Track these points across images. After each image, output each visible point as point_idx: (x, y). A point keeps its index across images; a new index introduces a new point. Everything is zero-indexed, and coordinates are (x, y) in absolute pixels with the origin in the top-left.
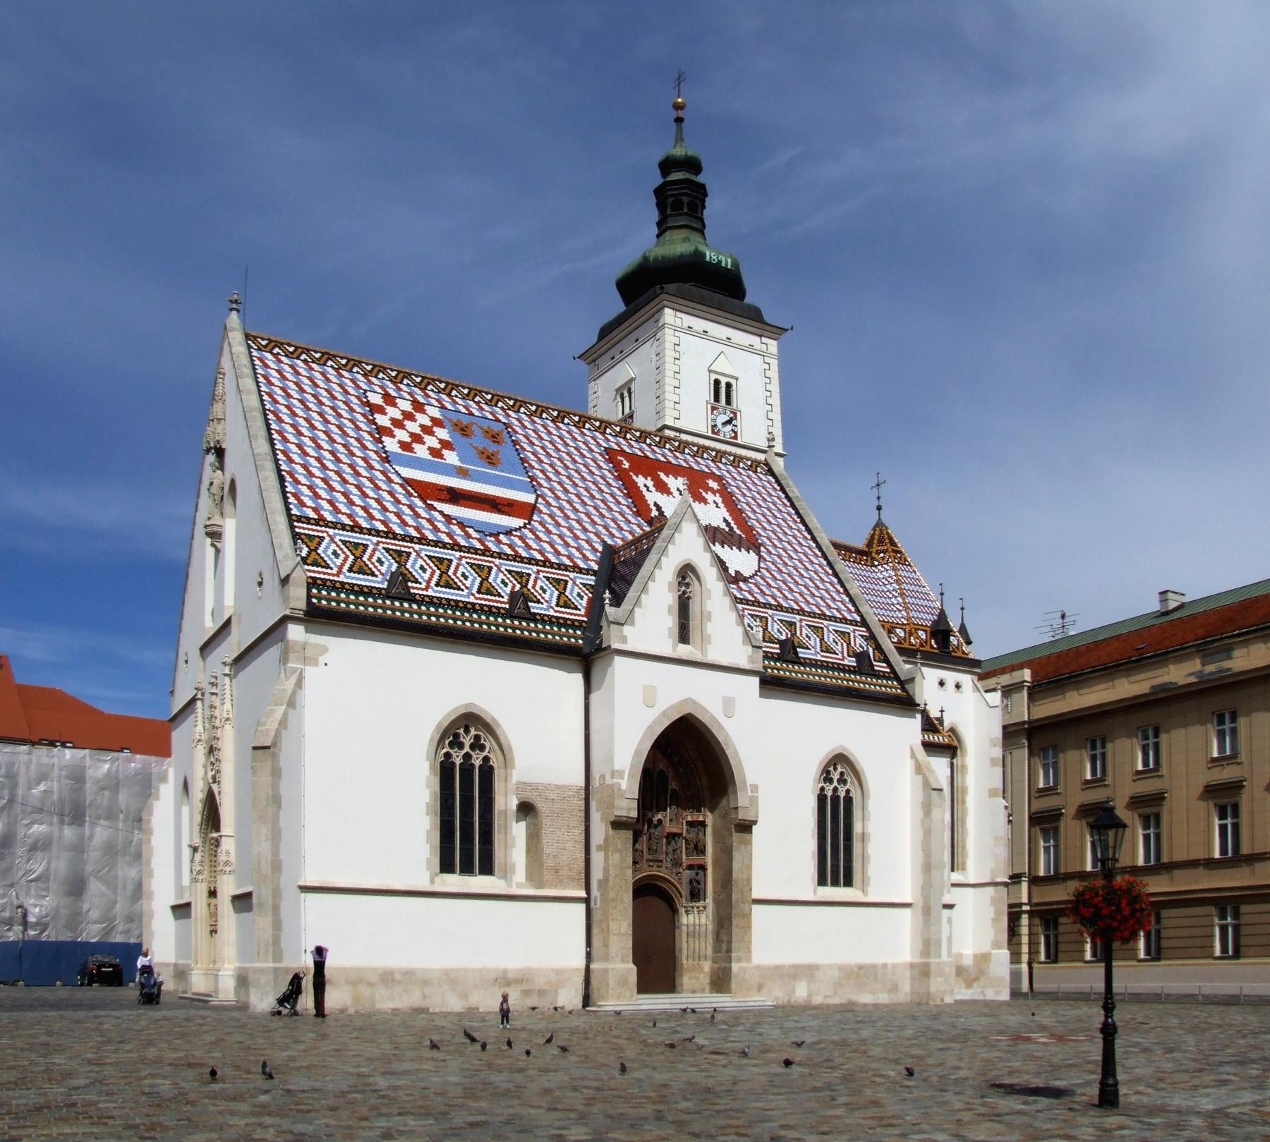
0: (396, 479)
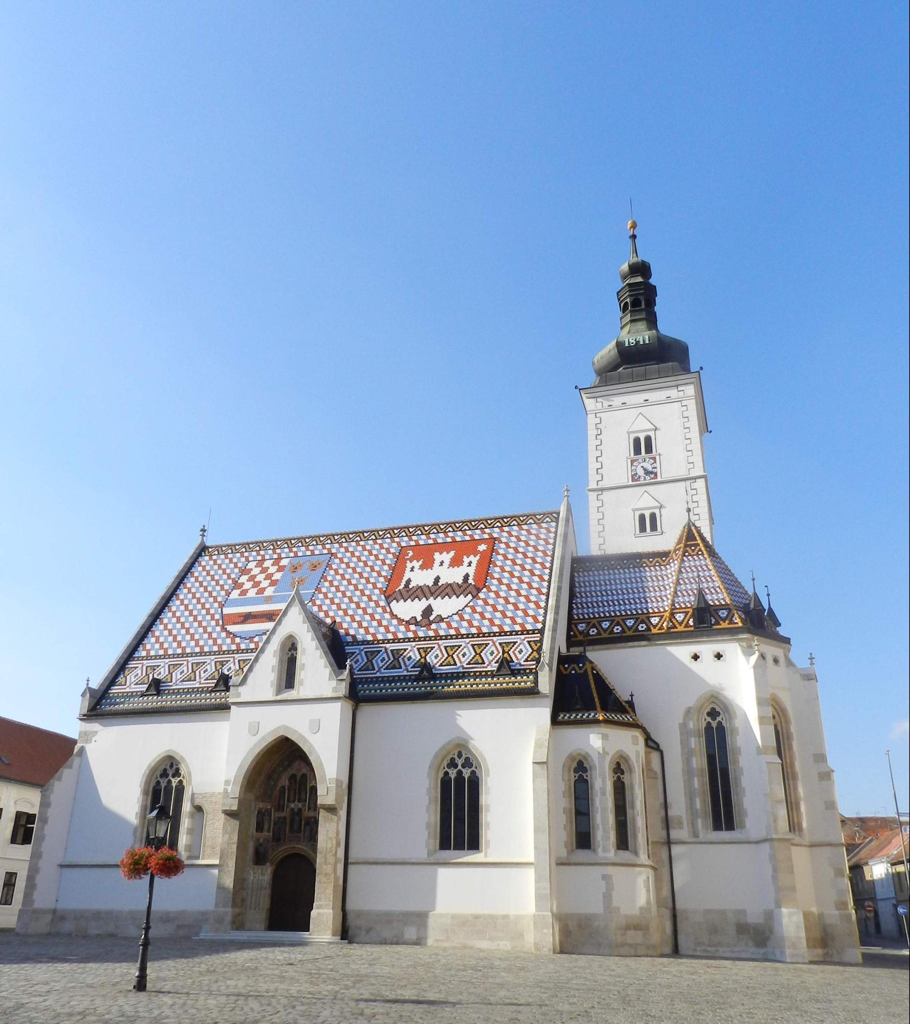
0: (217, 617)
